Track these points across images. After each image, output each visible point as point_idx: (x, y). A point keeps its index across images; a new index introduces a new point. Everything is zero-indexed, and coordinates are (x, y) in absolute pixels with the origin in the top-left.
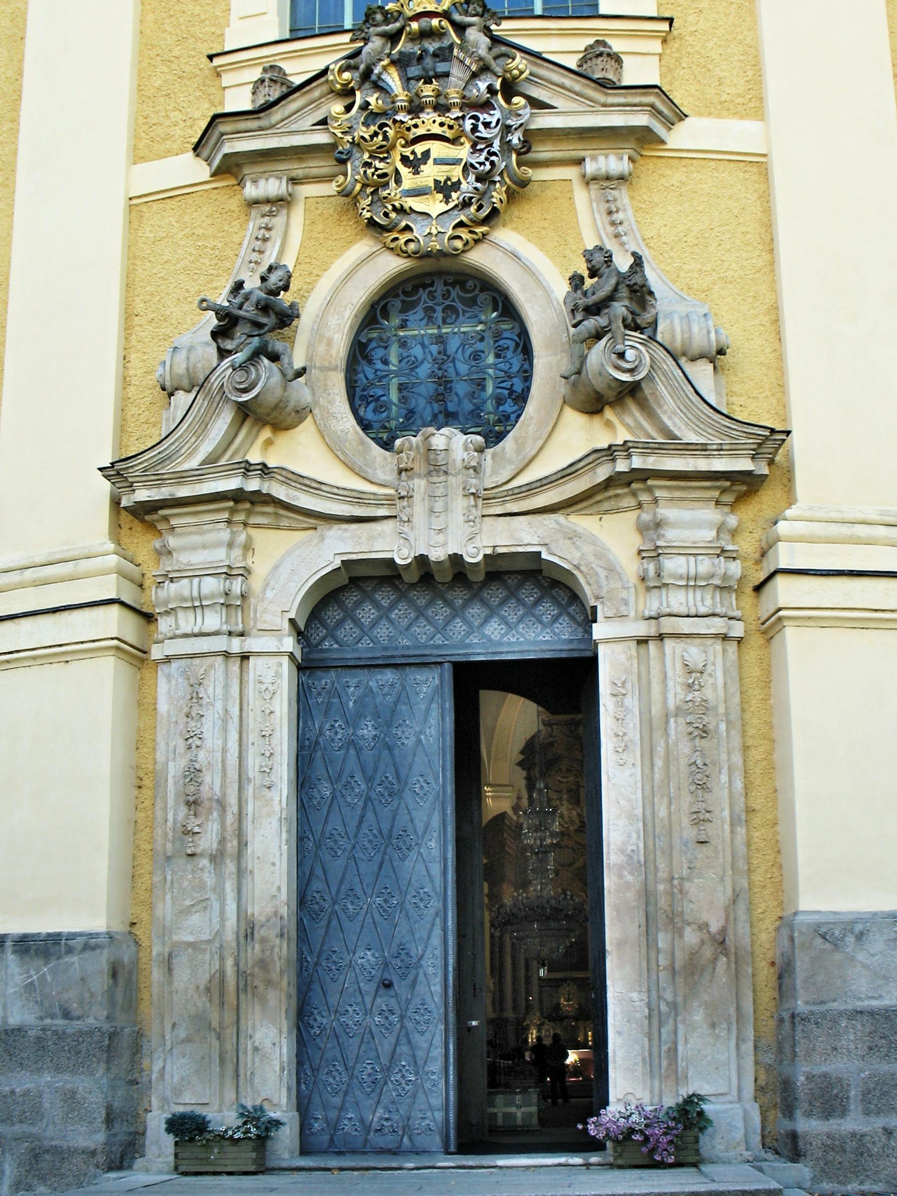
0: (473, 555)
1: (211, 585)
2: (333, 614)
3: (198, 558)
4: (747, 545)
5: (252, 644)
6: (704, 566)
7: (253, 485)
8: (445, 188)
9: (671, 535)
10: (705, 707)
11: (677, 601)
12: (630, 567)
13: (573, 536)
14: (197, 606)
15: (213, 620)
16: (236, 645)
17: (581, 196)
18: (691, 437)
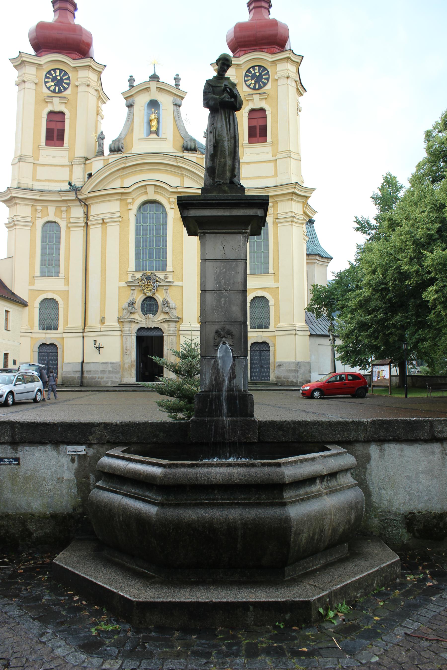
0: (152, 327)
1: (128, 329)
2: (139, 331)
3: (127, 326)
4: (178, 326)
5: (132, 335)
6: (174, 329)
7: (132, 320)
8: (150, 290)
9: (171, 326)
10: (173, 342)
11: (171, 332)
12: (167, 328)
13: (162, 326)
14: (127, 331)
15: (128, 333)
16: (130, 335)
17: (164, 291)
18: (173, 317)
